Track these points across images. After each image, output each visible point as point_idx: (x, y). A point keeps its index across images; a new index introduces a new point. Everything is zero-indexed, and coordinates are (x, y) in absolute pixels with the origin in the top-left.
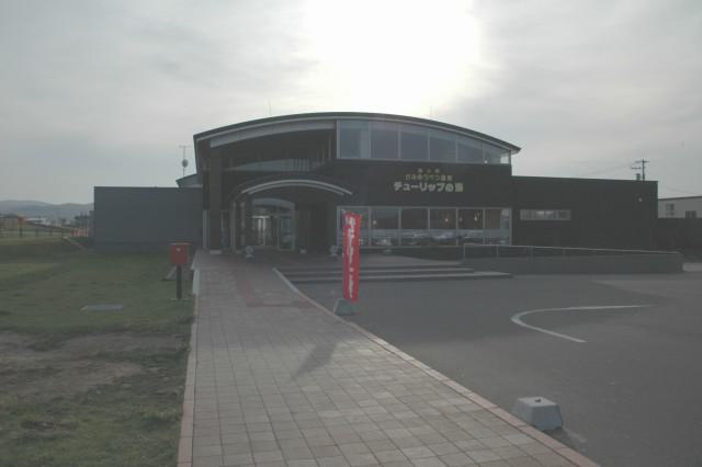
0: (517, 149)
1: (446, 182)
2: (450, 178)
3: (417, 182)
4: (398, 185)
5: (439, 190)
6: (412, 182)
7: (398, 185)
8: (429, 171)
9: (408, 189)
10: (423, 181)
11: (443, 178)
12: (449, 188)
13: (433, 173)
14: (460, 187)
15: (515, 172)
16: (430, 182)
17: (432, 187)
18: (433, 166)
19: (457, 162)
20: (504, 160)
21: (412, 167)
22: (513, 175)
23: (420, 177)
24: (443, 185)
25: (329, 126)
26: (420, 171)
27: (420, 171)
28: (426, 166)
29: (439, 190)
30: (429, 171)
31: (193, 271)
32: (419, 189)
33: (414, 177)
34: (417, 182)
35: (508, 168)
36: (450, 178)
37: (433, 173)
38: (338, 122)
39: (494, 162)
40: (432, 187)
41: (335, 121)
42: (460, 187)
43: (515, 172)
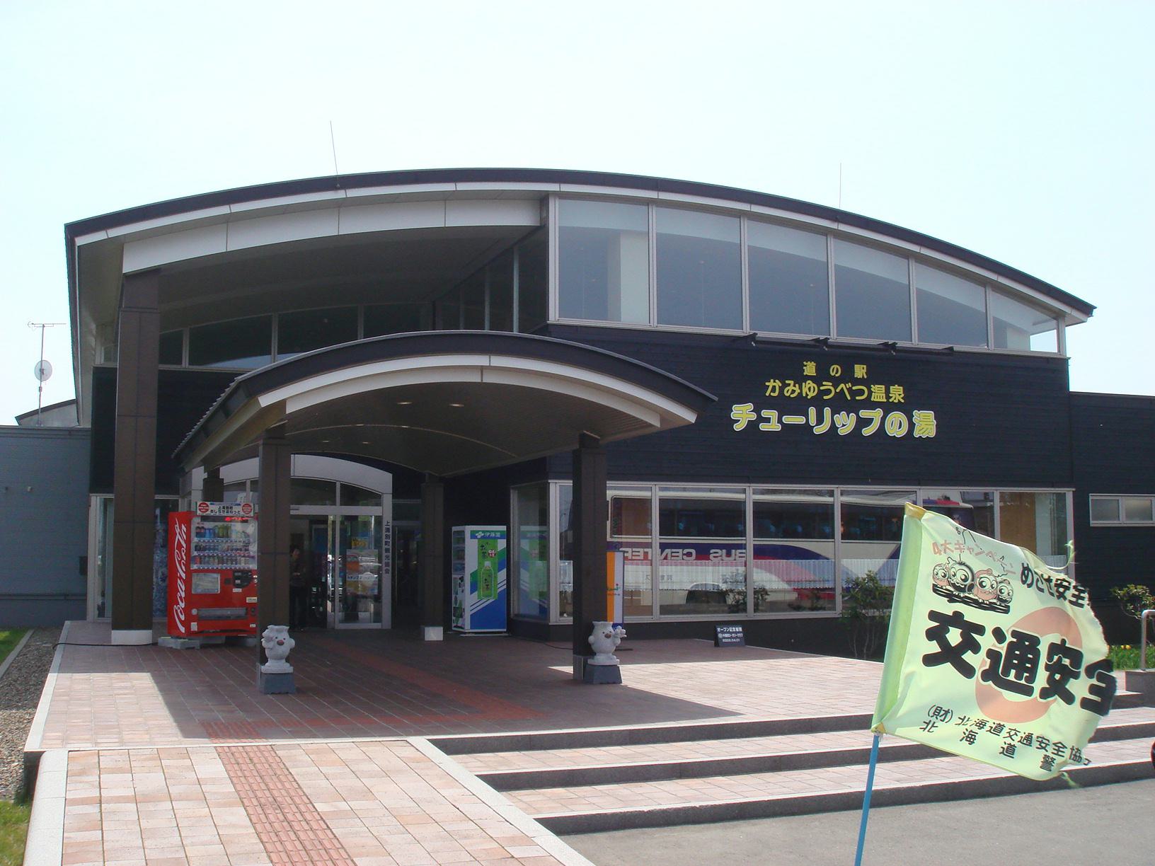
0: (1086, 309)
1: (888, 407)
2: (897, 393)
3: (799, 405)
4: (742, 414)
5: (867, 432)
6: (785, 405)
7: (742, 414)
8: (835, 371)
9: (774, 426)
10: (819, 402)
11: (878, 393)
12: (896, 426)
13: (848, 376)
14: (926, 424)
15: (1080, 381)
16: (840, 404)
17: (845, 423)
18: (848, 356)
19: (915, 342)
20: (1042, 343)
21: (785, 359)
22: (1071, 389)
23: (809, 389)
24: (877, 414)
25: (520, 218)
26: (810, 369)
27: (810, 369)
28: (823, 352)
29: (867, 432)
30: (835, 371)
31: (32, 764)
32: (807, 428)
33: (792, 390)
34: (799, 405)
35: (1056, 367)
36: (897, 393)
37: (848, 376)
38: (554, 207)
39: (1013, 346)
40: (845, 423)
41: (542, 201)
42: (926, 424)
43: (1080, 381)
